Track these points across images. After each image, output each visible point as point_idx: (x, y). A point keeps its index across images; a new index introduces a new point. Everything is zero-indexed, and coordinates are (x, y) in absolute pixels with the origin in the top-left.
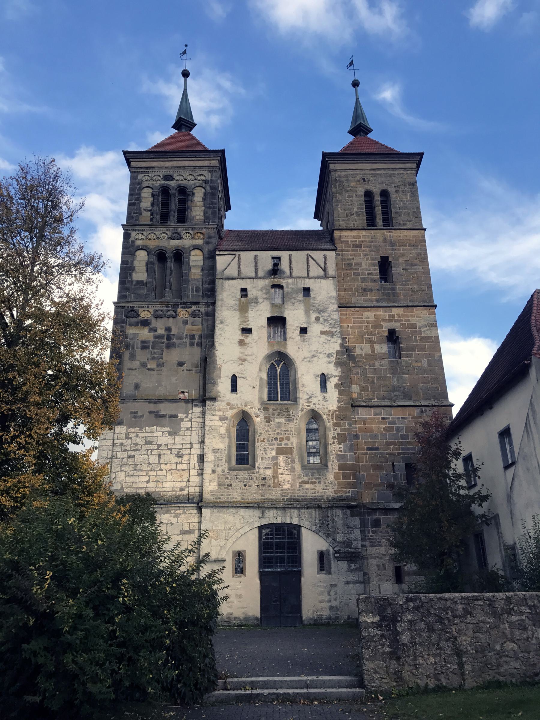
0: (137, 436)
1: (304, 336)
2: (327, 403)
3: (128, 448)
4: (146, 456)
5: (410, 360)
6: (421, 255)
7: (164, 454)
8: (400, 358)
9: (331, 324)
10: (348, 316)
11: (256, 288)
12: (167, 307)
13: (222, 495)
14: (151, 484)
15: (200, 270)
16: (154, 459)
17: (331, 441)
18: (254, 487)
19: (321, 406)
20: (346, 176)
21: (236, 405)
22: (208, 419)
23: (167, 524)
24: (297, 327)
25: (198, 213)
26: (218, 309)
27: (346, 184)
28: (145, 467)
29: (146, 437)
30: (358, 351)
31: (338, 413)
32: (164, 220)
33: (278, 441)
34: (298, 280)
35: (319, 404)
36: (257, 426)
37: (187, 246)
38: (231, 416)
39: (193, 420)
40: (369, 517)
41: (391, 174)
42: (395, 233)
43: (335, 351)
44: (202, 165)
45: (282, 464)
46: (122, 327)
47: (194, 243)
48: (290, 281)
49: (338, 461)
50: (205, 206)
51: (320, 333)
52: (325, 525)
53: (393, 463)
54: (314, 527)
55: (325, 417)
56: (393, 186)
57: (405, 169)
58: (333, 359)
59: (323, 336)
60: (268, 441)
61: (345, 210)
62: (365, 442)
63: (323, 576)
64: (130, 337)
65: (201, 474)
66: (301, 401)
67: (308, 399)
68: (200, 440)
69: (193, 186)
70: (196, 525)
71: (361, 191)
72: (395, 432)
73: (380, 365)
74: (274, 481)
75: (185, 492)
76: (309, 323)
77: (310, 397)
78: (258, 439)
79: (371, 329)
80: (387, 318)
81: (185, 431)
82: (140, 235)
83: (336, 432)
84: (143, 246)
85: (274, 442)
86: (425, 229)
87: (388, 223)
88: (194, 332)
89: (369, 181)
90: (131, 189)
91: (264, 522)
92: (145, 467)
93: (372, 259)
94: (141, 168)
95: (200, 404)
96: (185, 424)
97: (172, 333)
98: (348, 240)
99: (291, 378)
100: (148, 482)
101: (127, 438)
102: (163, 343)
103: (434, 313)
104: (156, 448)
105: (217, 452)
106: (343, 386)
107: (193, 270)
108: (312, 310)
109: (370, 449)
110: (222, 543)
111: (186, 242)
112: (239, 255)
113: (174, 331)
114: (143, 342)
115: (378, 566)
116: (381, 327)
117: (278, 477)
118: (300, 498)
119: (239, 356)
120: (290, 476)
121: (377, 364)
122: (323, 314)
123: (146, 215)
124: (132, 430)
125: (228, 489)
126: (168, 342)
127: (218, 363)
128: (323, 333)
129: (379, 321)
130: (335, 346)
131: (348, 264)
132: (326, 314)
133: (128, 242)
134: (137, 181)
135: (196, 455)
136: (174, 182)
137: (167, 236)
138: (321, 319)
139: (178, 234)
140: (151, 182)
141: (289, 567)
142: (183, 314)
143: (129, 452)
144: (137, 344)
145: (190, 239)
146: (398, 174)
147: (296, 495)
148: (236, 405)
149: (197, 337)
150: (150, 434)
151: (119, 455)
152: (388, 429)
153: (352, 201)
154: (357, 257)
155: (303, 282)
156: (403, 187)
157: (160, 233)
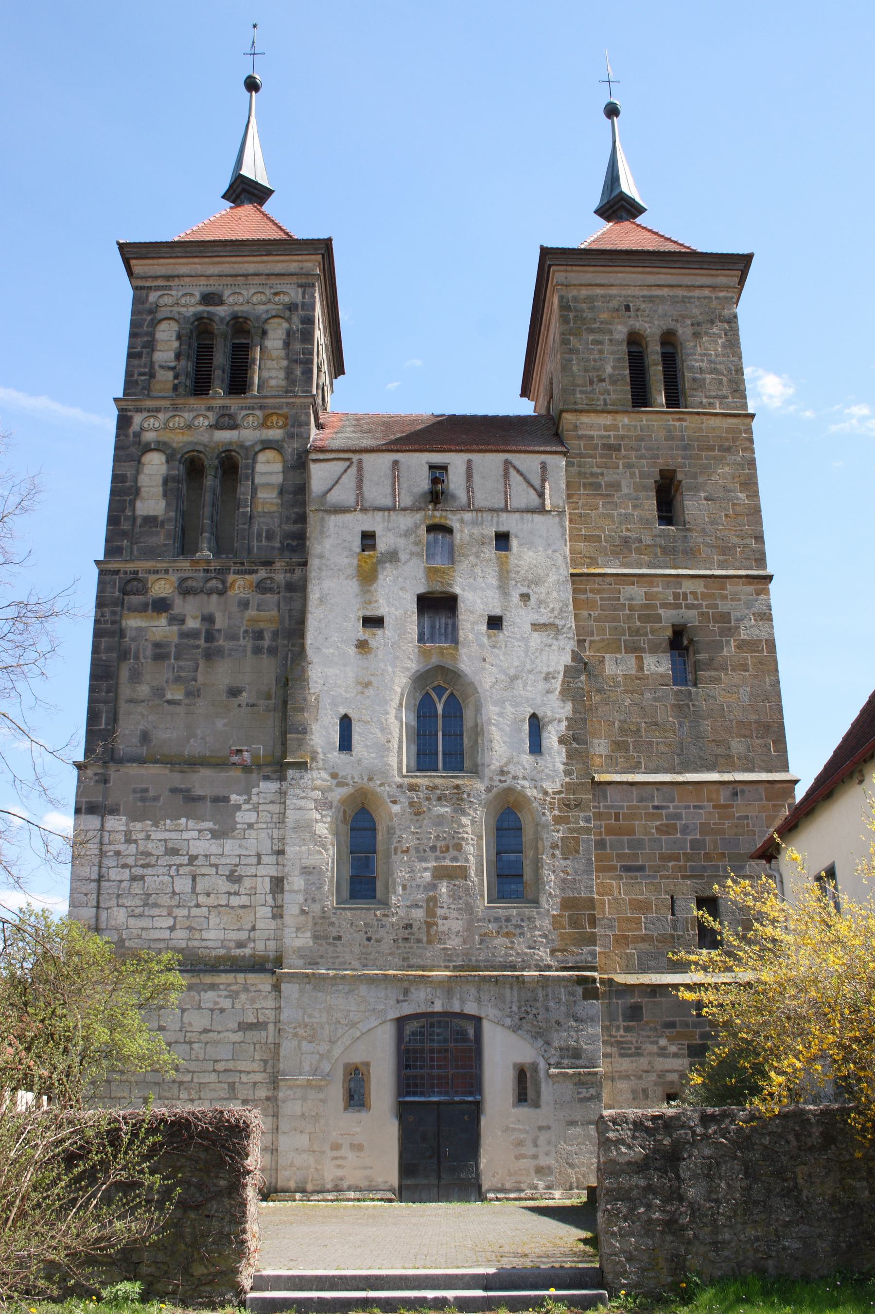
0: (148, 837)
3: (131, 861)
4: (167, 879)
7: (203, 875)
8: (695, 685)
10: (590, 595)
11: (396, 532)
12: (207, 571)
13: (321, 957)
14: (180, 934)
15: (274, 494)
16: (183, 885)
18: (388, 941)
20: (590, 299)
21: (349, 777)
22: (292, 807)
23: (212, 1010)
25: (273, 373)
26: (313, 574)
27: (588, 315)
28: (165, 900)
29: (165, 840)
31: (563, 795)
32: (200, 386)
33: (438, 853)
35: (524, 778)
37: (248, 444)
38: (339, 801)
39: (261, 808)
40: (620, 1002)
41: (684, 297)
42: (690, 423)
43: (562, 669)
44: (283, 271)
45: (445, 898)
46: (114, 613)
47: (264, 437)
48: (468, 516)
50: (287, 357)
52: (531, 1016)
56: (689, 322)
57: (713, 287)
58: (557, 684)
59: (535, 635)
60: (417, 850)
61: (586, 371)
62: (618, 856)
63: (524, 1111)
64: (129, 634)
65: (278, 913)
66: (486, 770)
67: (501, 767)
68: (276, 848)
69: (264, 316)
70: (271, 1015)
71: (621, 331)
72: (679, 835)
74: (428, 932)
75: (247, 951)
76: (505, 608)
77: (506, 765)
78: (396, 849)
79: (638, 624)
81: (244, 830)
82: (152, 420)
84: (159, 442)
85: (429, 853)
86: (752, 416)
88: (262, 625)
89: (638, 310)
90: (134, 324)
91: (407, 1009)
92: (165, 900)
93: (642, 475)
94: (156, 278)
95: (275, 776)
96: (244, 817)
98: (591, 433)
99: (468, 723)
100: (172, 929)
101: (129, 841)
102: (198, 647)
103: (767, 592)
104: (186, 862)
105: (310, 873)
106: (576, 741)
107: (261, 495)
110: (323, 1048)
112: (360, 461)
113: (220, 623)
114: (157, 645)
115: (634, 1092)
116: (658, 619)
117: (436, 924)
119: (357, 678)
120: (460, 922)
122: (535, 589)
123: (165, 377)
124: (138, 826)
125: (335, 946)
126: (208, 645)
127: (312, 691)
129: (654, 606)
130: (559, 657)
131: (591, 484)
133: (127, 436)
134: (147, 306)
135: (268, 879)
136: (225, 308)
137: (206, 423)
139: (230, 416)
140: (176, 309)
141: (457, 1093)
142: (240, 586)
143: (133, 870)
144: (144, 650)
145: (255, 428)
146: (699, 298)
147: (474, 959)
148: (349, 777)
149: (267, 636)
150: (174, 835)
151: (114, 874)
152: (665, 829)
153: (601, 352)
155: (495, 519)
156: (709, 326)
157: (192, 415)
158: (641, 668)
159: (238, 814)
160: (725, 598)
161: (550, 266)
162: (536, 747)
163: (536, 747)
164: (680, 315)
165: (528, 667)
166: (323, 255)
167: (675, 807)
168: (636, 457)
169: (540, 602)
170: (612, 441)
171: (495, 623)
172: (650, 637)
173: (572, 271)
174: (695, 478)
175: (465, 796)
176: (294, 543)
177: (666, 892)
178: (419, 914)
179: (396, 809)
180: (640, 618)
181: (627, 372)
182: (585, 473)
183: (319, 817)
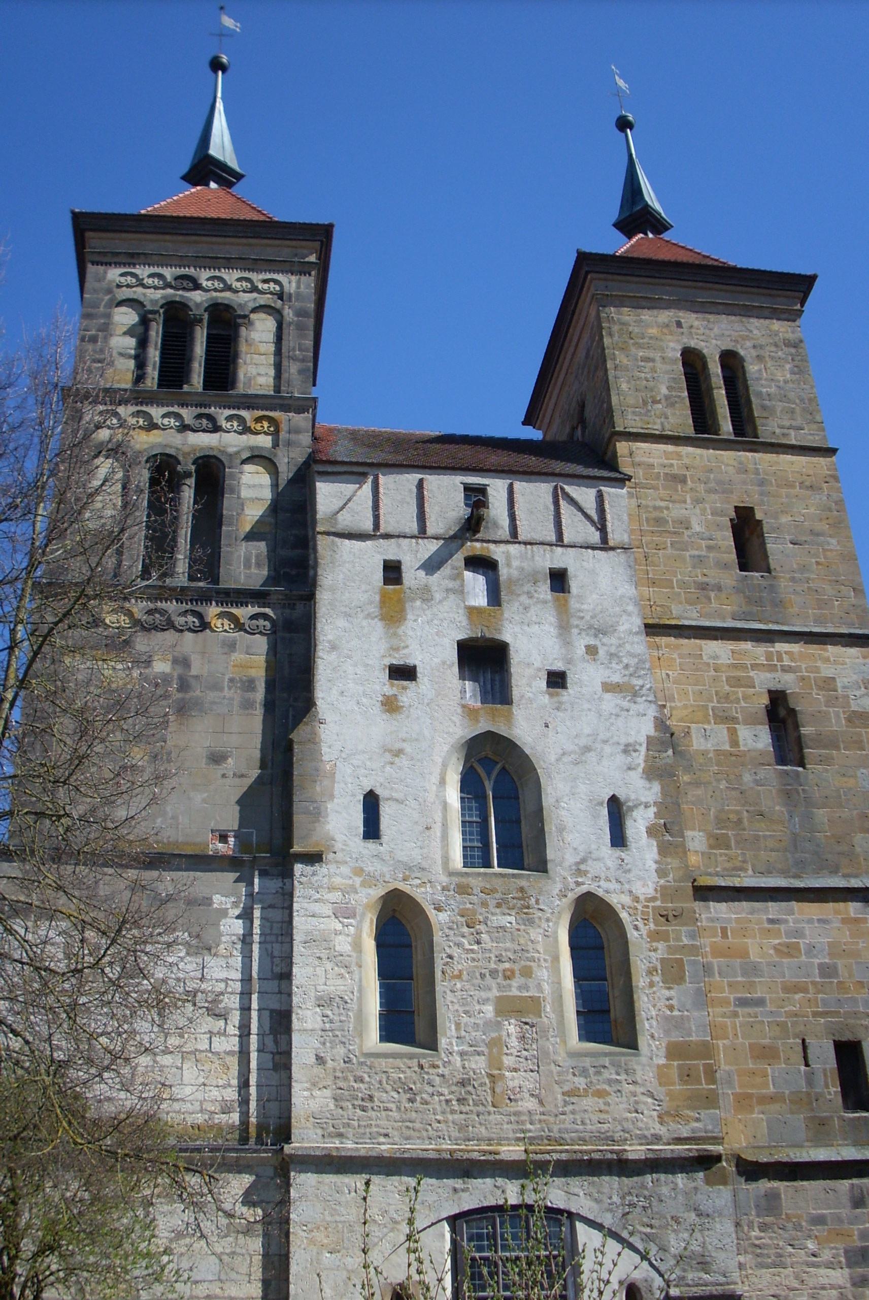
1: (558, 694)
2: (628, 876)
5: (827, 770)
6: (830, 510)
8: (802, 764)
9: (627, 667)
17: (640, 980)
19: (613, 886)
24: (539, 670)
25: (262, 370)
30: (697, 743)
34: (535, 547)
35: (608, 880)
36: (438, 937)
37: (231, 450)
43: (643, 739)
48: (513, 549)
49: (667, 1032)
51: (599, 688)
53: (804, 1041)
54: (609, 1215)
55: (624, 915)
56: (748, 344)
58: (640, 758)
59: (608, 696)
67: (578, 864)
68: (277, 970)
69: (251, 305)
72: (803, 958)
73: (757, 783)
76: (569, 661)
77: (583, 861)
79: (727, 688)
80: (763, 660)
83: (659, 955)
87: (745, 432)
91: (468, 1202)
97: (194, 672)
98: (651, 460)
108: (577, 626)
109: (743, 1002)
111: (230, 441)
118: (566, 1136)
119: (385, 743)
121: (747, 778)
122: (605, 640)
126: (180, 695)
127: (325, 758)
128: (608, 687)
132: (614, 641)
138: (602, 652)
147: (556, 1128)
152: (786, 950)
153: (653, 370)
154: (677, 505)
156: (773, 349)
158: (734, 743)
159: (223, 921)
160: (827, 660)
161: (587, 273)
162: (618, 839)
163: (618, 839)
164: (740, 336)
165: (602, 736)
166: (322, 242)
167: (796, 921)
168: (706, 491)
169: (612, 655)
170: (675, 471)
171: (557, 680)
172: (743, 704)
173: (613, 280)
174: (776, 518)
175: (533, 901)
176: (294, 572)
177: (796, 1036)
178: (479, 1064)
179: (443, 917)
180: (728, 679)
181: (686, 394)
182: (647, 506)
183: (339, 927)
